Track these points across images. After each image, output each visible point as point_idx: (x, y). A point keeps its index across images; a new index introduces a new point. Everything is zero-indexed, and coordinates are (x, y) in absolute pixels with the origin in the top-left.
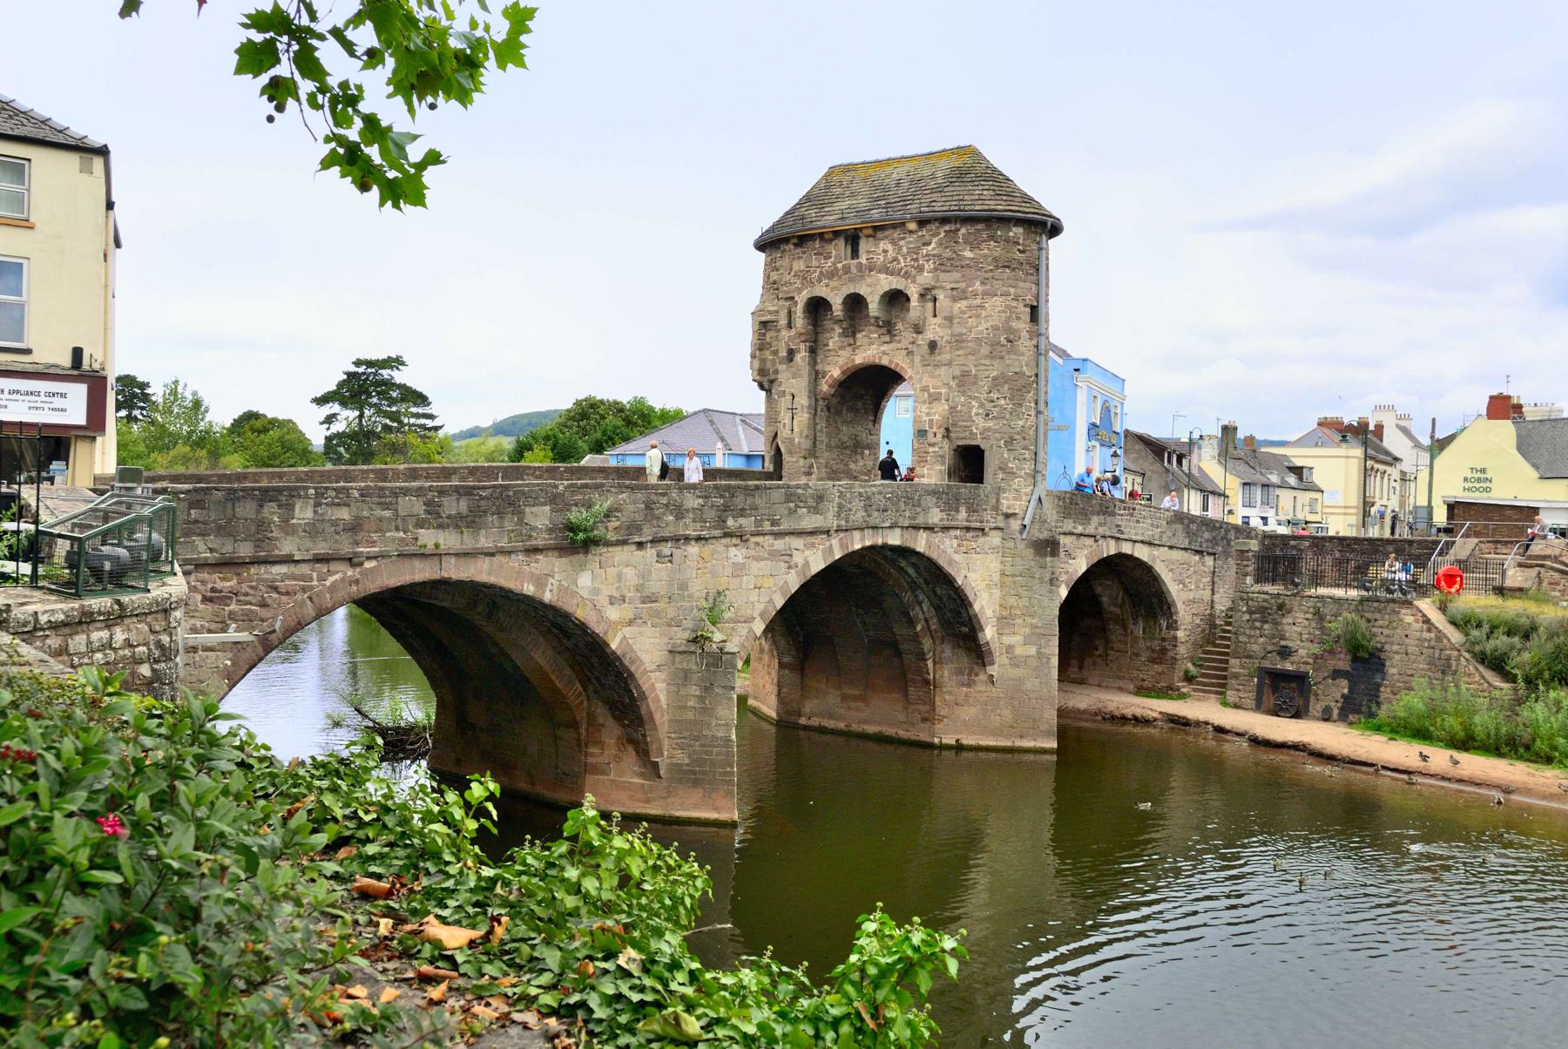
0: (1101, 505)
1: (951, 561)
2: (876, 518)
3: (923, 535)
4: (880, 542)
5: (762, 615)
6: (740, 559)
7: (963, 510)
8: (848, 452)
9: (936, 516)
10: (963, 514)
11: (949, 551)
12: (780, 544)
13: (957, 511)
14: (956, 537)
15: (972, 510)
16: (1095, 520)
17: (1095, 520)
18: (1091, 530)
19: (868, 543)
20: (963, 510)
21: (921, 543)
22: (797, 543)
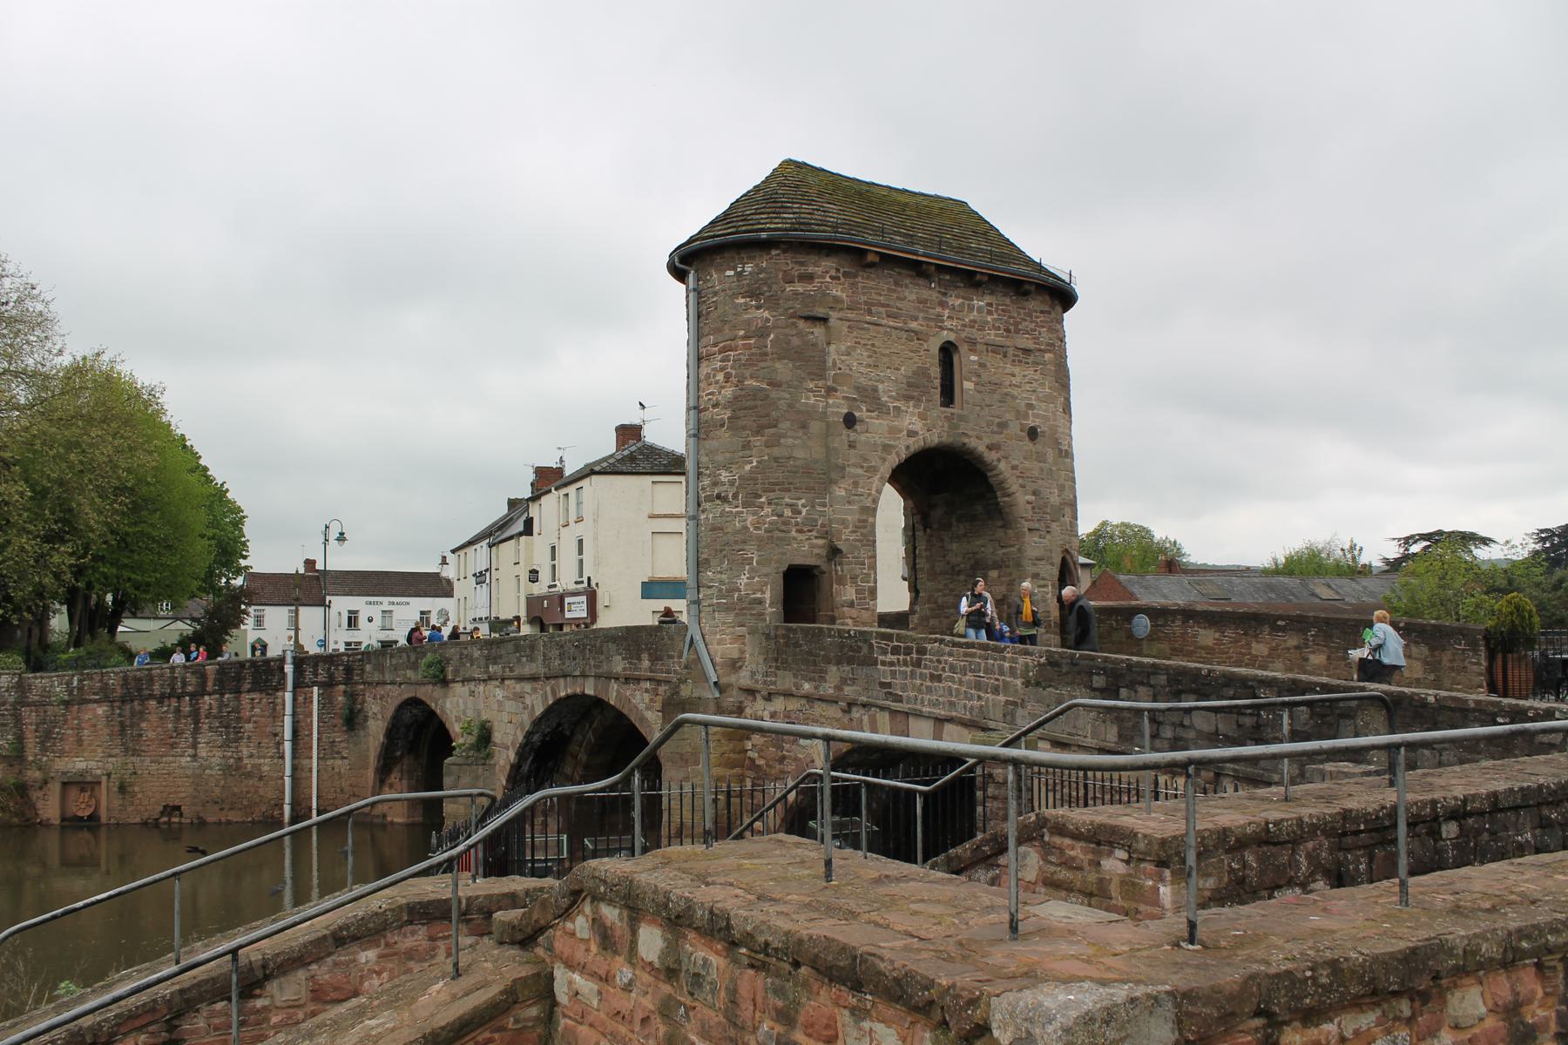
0: (842, 646)
1: (643, 719)
2: (569, 666)
3: (614, 686)
4: (578, 691)
5: (513, 744)
6: (500, 698)
7: (645, 656)
8: (962, 577)
9: (619, 665)
10: (646, 663)
11: (642, 706)
12: (518, 687)
13: (639, 659)
14: (647, 691)
15: (655, 658)
16: (833, 673)
17: (833, 673)
18: (828, 689)
19: (570, 691)
20: (645, 656)
21: (613, 694)
22: (527, 687)
